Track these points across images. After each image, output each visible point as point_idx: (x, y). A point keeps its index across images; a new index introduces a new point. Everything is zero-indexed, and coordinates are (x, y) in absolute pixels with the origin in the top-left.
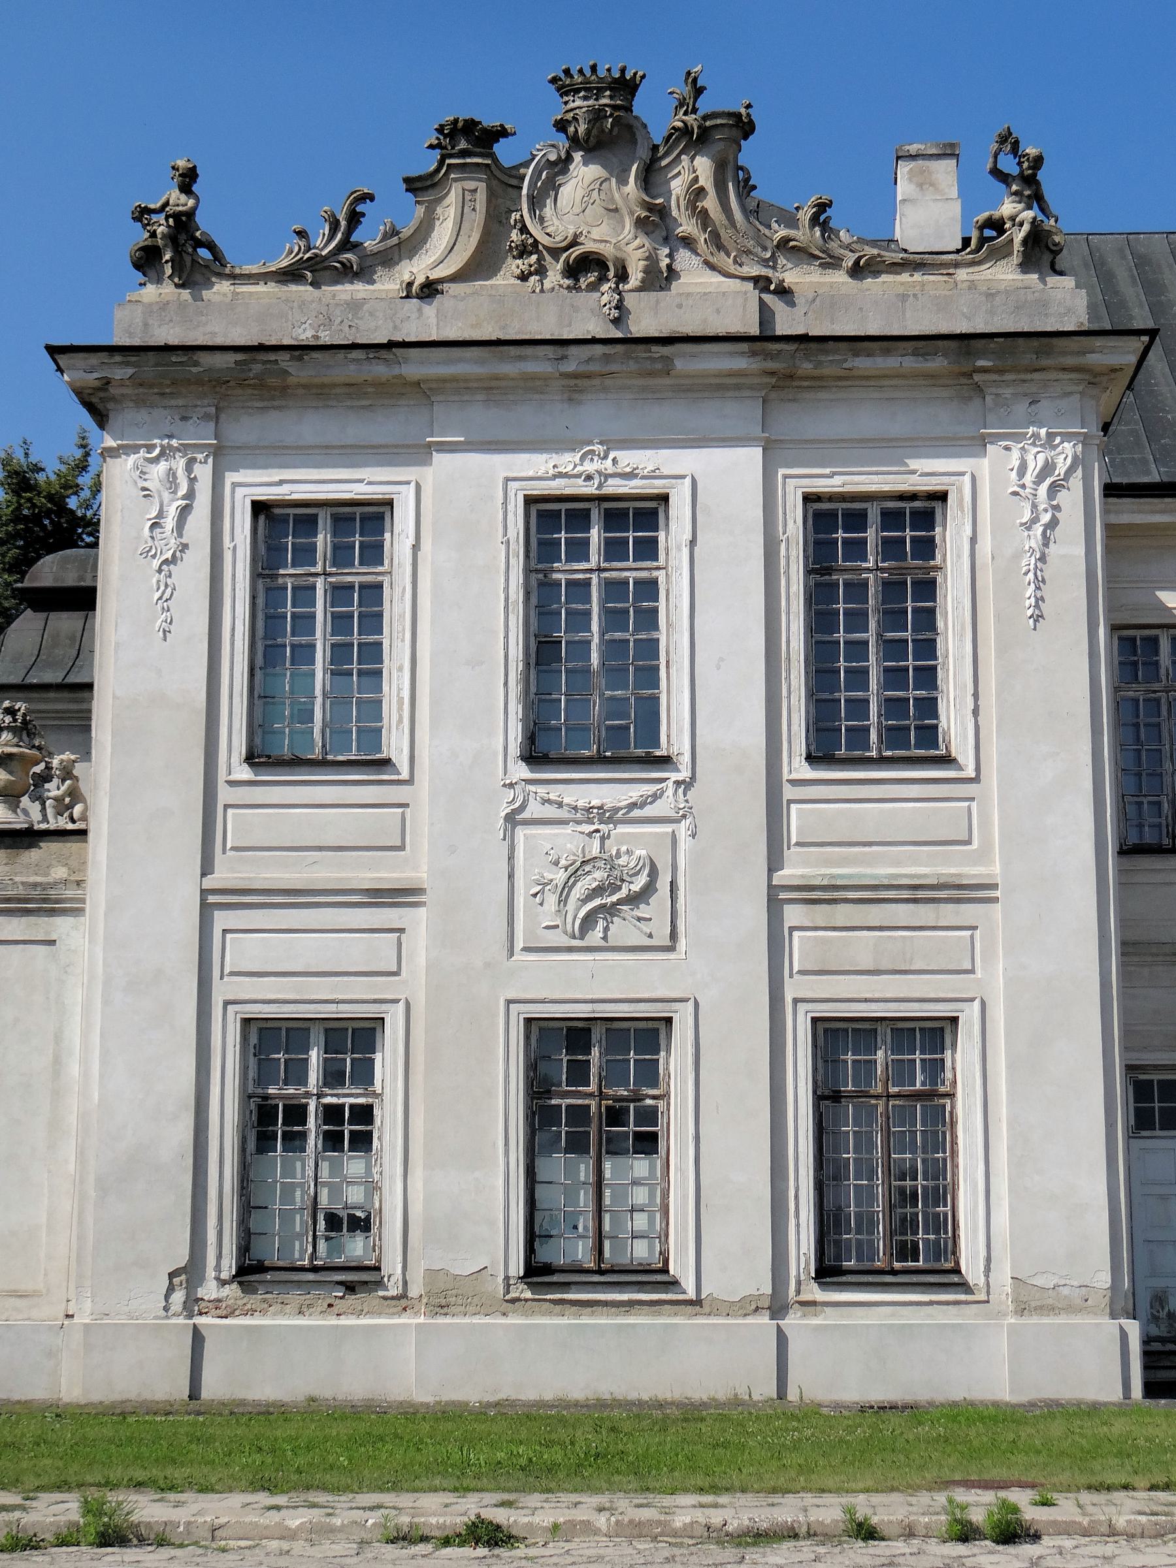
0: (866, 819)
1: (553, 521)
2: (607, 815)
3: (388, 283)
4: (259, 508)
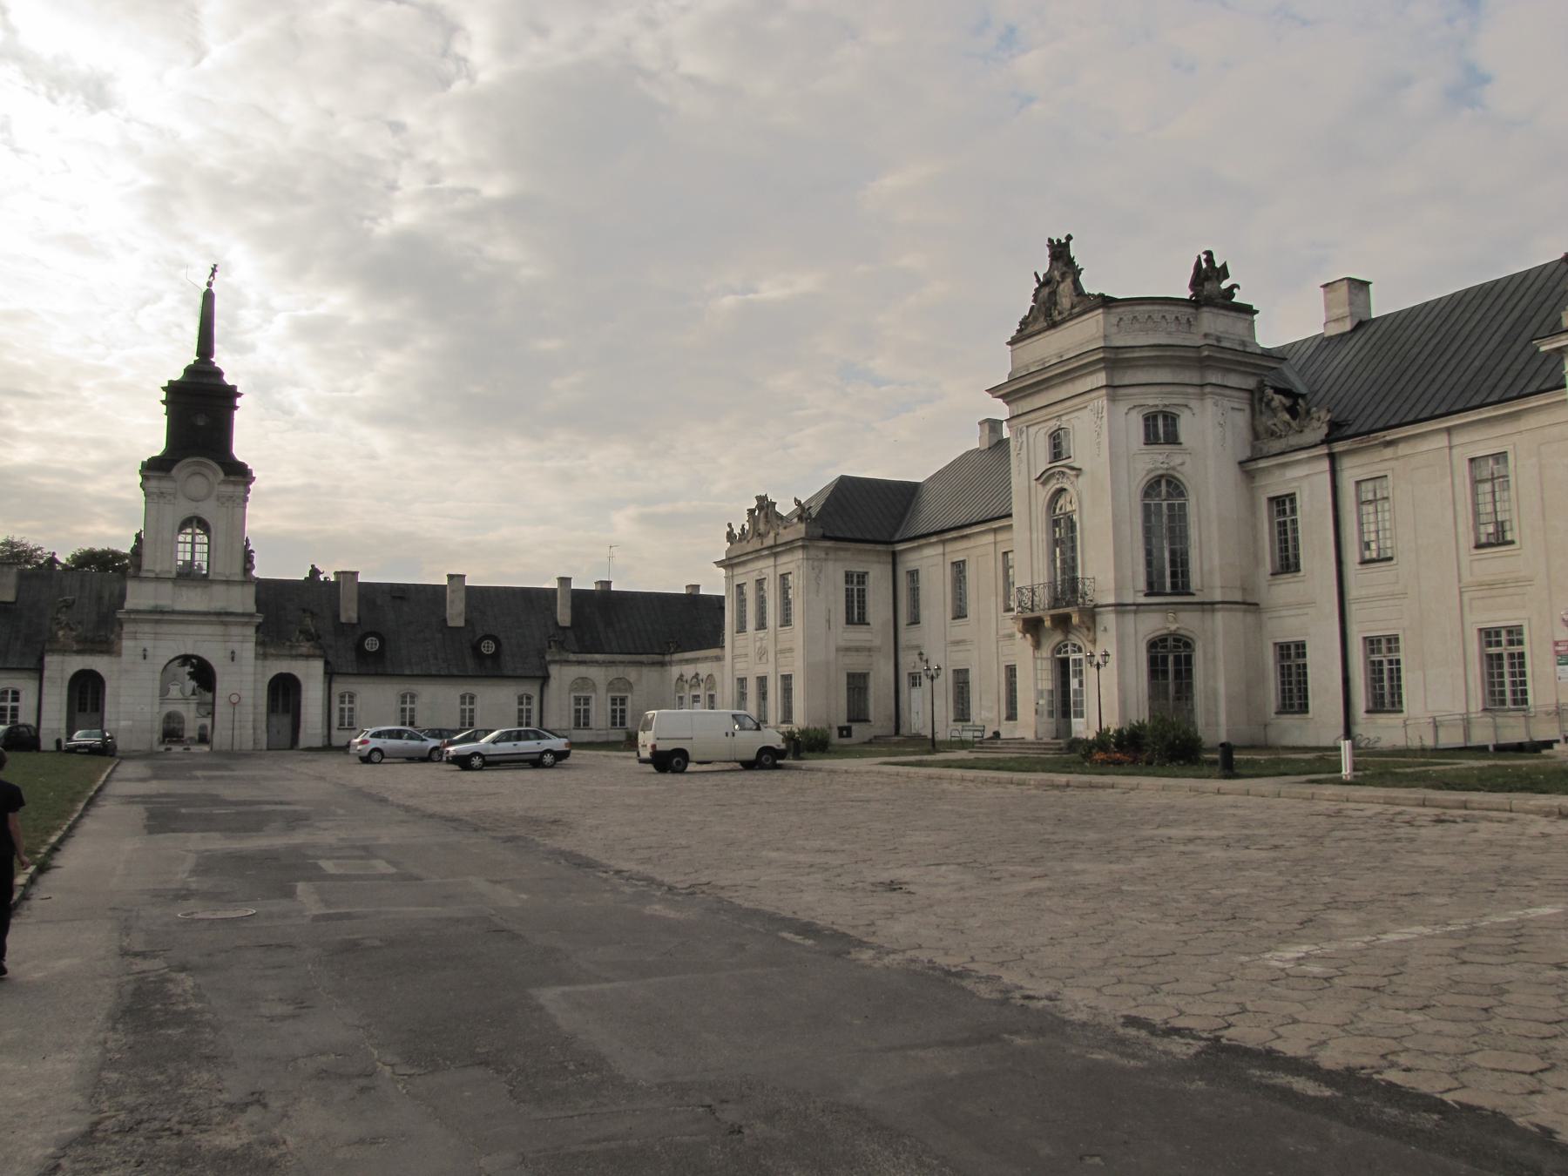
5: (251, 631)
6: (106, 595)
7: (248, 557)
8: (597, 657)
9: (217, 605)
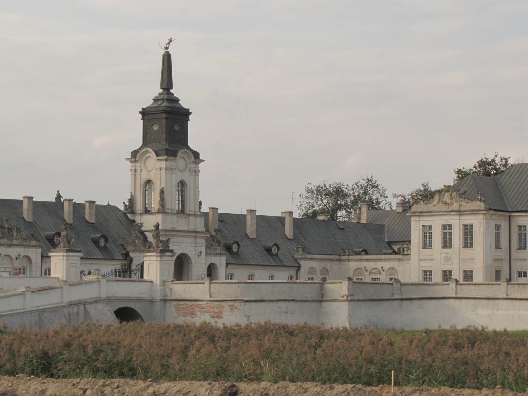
0: (468, 252)
1: (444, 227)
2: (447, 253)
3: (431, 205)
4: (423, 226)
5: (203, 241)
6: (120, 219)
7: (200, 203)
8: (317, 256)
9: (192, 228)
